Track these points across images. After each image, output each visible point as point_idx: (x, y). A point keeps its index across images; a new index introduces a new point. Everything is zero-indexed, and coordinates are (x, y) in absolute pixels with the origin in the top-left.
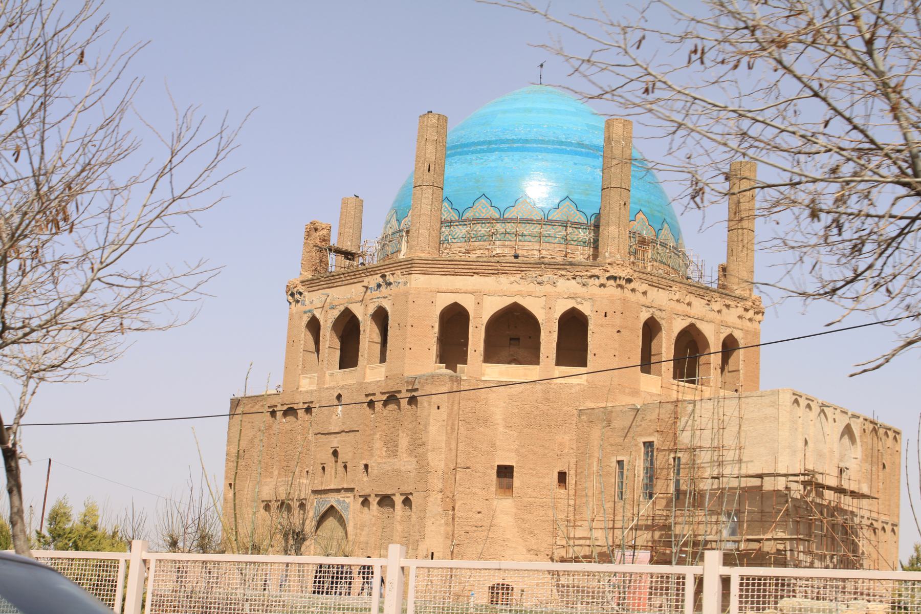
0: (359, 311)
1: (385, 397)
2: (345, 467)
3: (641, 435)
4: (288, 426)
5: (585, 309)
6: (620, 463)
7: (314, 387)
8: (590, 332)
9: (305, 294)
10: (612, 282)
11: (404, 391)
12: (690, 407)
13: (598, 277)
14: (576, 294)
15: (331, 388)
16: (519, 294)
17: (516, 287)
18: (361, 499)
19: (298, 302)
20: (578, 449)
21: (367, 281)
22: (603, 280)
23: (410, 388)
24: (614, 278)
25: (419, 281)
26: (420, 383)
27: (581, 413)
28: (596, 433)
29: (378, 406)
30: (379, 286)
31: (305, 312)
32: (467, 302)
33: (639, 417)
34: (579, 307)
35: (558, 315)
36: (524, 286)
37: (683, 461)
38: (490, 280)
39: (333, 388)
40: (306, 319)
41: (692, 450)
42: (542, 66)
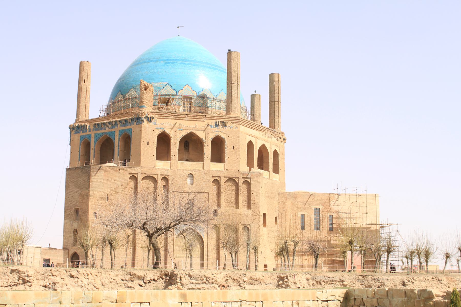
0: (201, 135)
1: (227, 179)
3: (313, 205)
4: (145, 185)
6: (303, 216)
9: (155, 118)
11: (241, 177)
12: (336, 197)
15: (183, 170)
18: (212, 226)
19: (151, 121)
20: (279, 208)
21: (206, 122)
23: (245, 177)
25: (242, 128)
26: (252, 175)
27: (280, 193)
28: (289, 202)
29: (222, 183)
30: (217, 125)
31: (157, 129)
33: (311, 197)
37: (334, 216)
39: (186, 170)
40: (157, 133)
41: (337, 212)
42: (178, 27)
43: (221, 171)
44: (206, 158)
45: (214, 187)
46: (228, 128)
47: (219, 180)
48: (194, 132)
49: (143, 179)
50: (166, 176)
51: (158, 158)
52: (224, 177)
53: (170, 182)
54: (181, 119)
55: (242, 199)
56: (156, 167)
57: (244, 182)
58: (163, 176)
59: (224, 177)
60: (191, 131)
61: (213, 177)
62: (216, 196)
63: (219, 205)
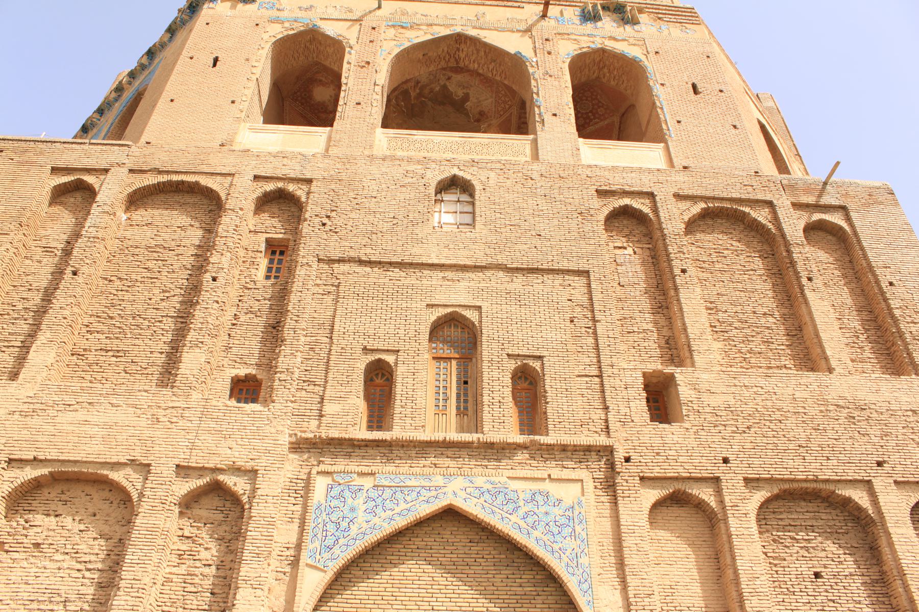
18: (652, 495)
23: (811, 200)
31: (272, 21)
39: (425, 162)
43: (650, 171)
44: (547, 117)
45: (625, 260)
47: (646, 210)
49: (137, 199)
50: (291, 187)
52: (678, 196)
55: (829, 307)
57: (811, 229)
58: (270, 187)
59: (678, 196)
60: (458, 29)
61: (602, 193)
62: (646, 304)
63: (676, 349)
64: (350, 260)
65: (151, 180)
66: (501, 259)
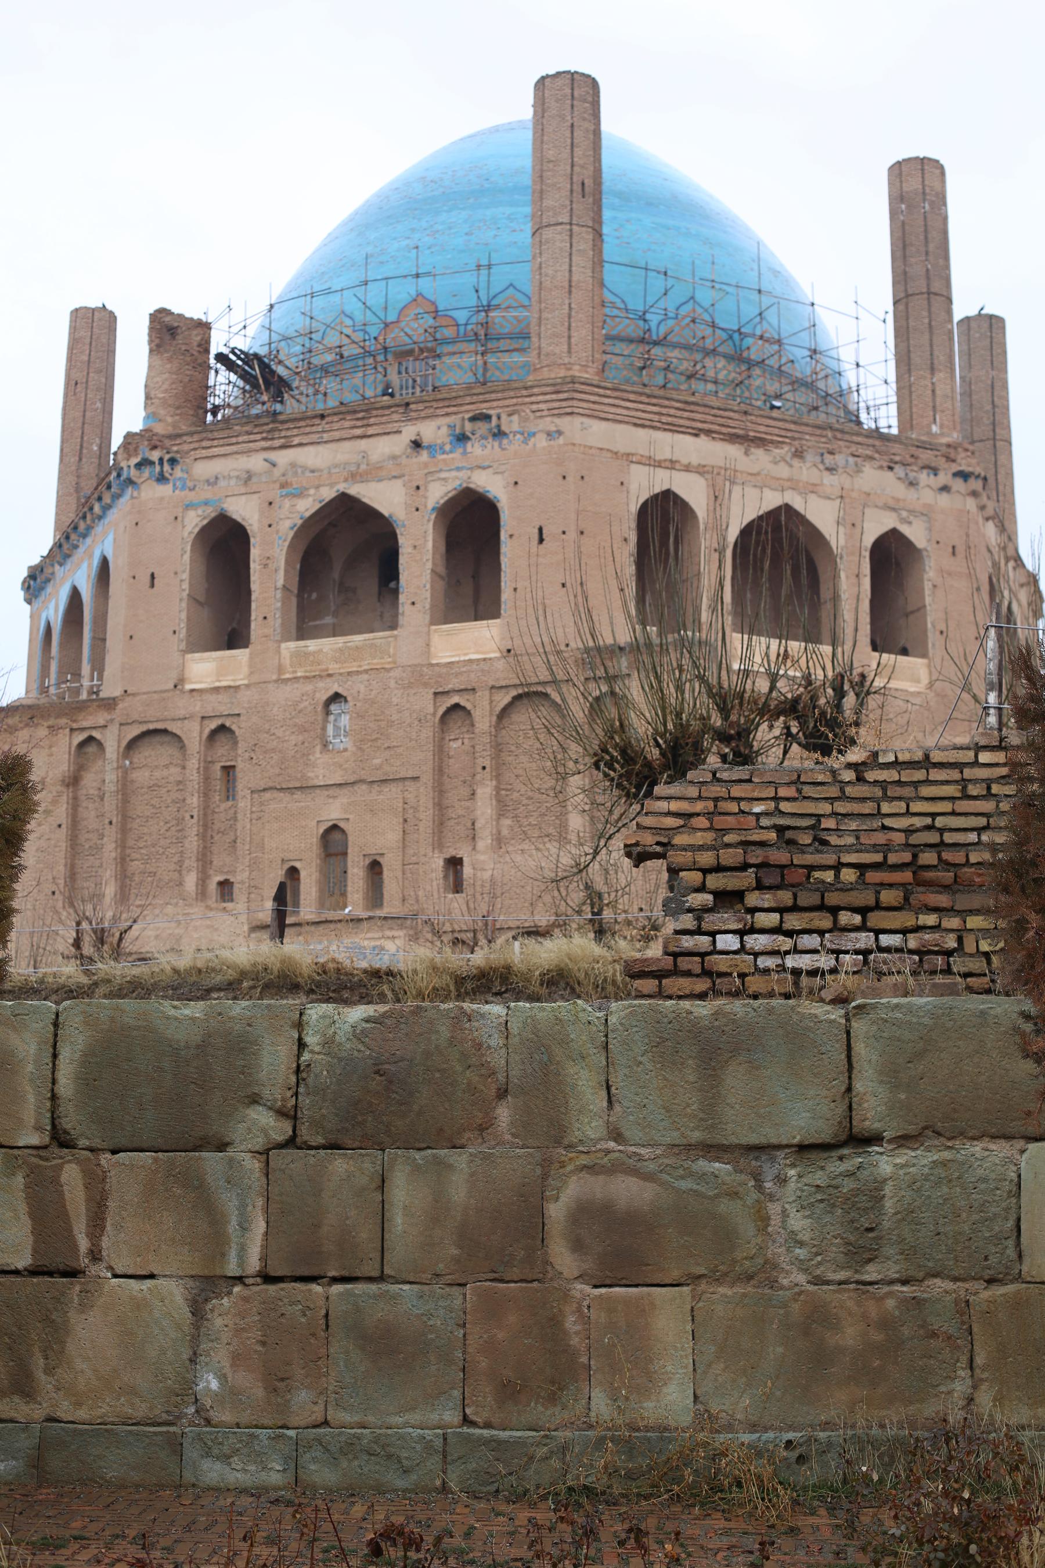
0: (385, 497)
2: (375, 867)
5: (915, 533)
7: (240, 678)
8: (928, 586)
10: (958, 484)
13: (935, 471)
14: (898, 500)
16: (793, 485)
17: (783, 471)
21: (409, 432)
22: (943, 478)
24: (964, 476)
31: (189, 507)
32: (694, 492)
34: (905, 529)
35: (869, 540)
36: (807, 471)
38: (734, 451)
40: (194, 521)
46: (514, 445)
48: (354, 490)
51: (200, 643)
53: (184, 738)
54: (296, 441)
56: (188, 687)
58: (213, 725)
60: (342, 487)
64: (271, 788)
65: (135, 731)
66: (363, 774)
